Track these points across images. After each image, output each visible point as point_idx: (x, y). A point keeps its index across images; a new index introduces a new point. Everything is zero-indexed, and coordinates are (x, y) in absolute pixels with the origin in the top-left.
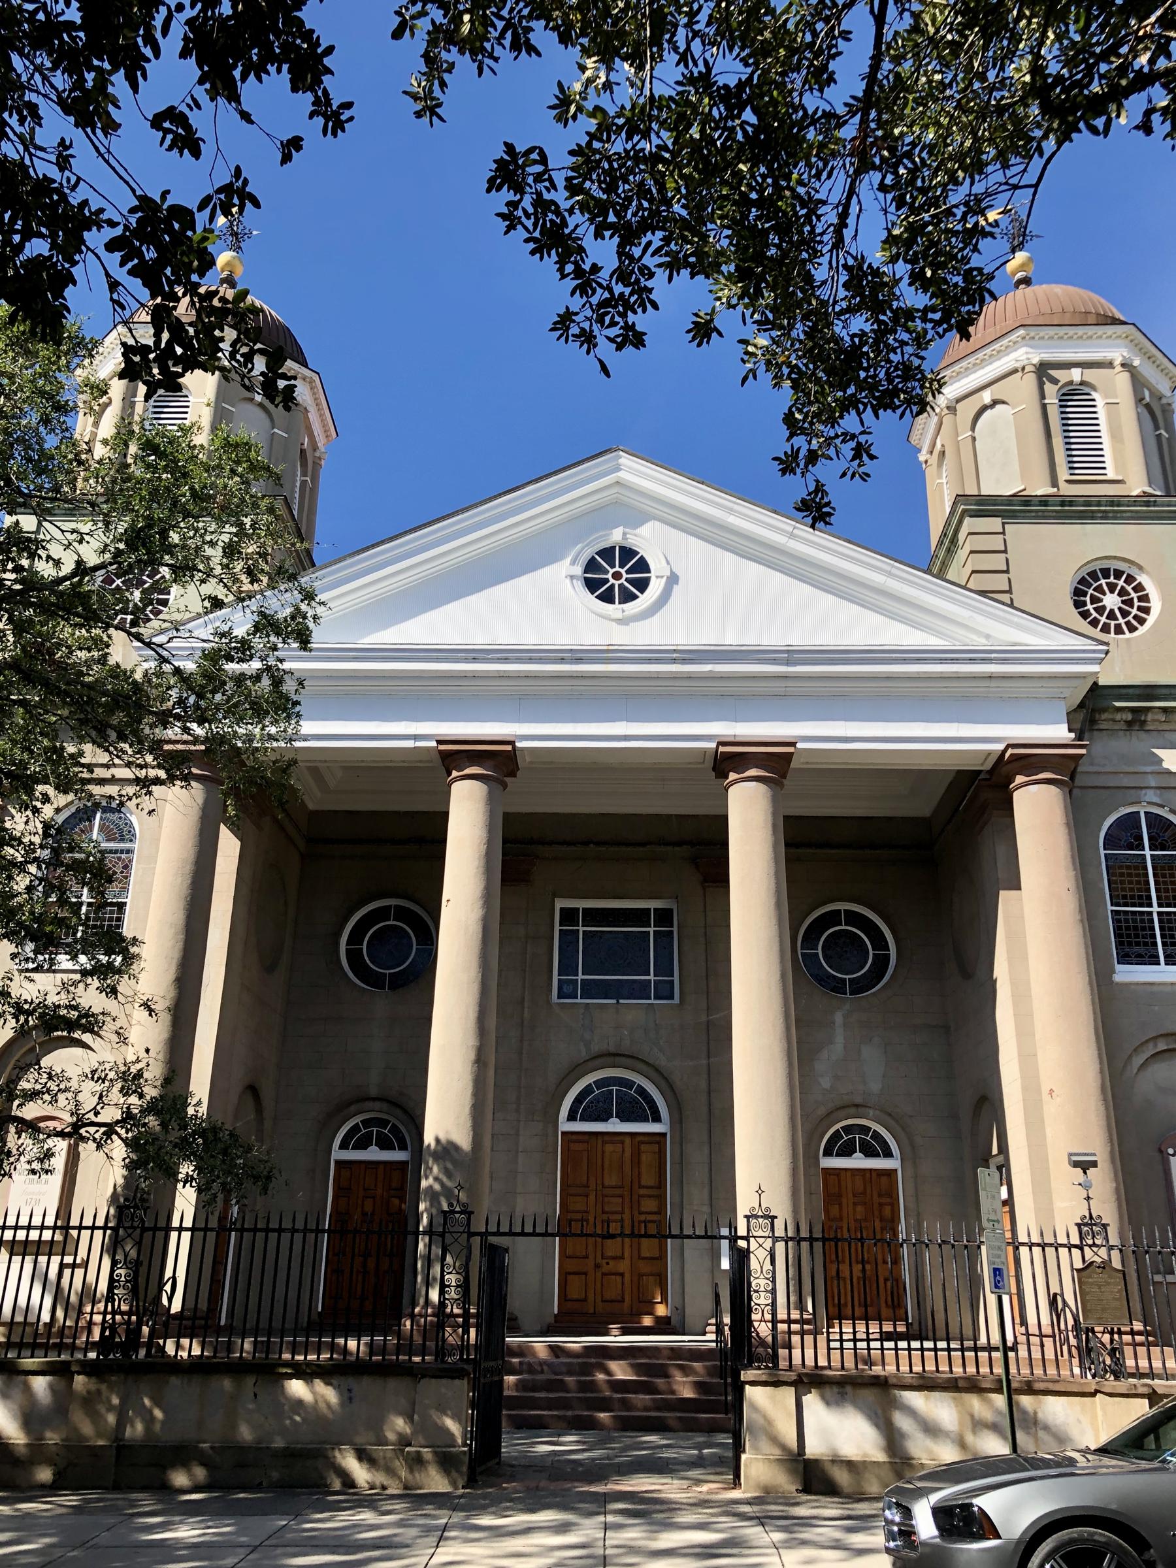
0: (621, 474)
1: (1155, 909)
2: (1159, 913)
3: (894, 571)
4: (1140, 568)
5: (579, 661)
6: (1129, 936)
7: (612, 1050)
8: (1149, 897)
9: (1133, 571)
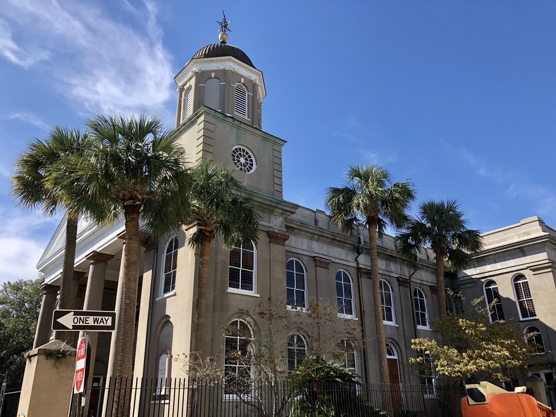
1: (241, 268)
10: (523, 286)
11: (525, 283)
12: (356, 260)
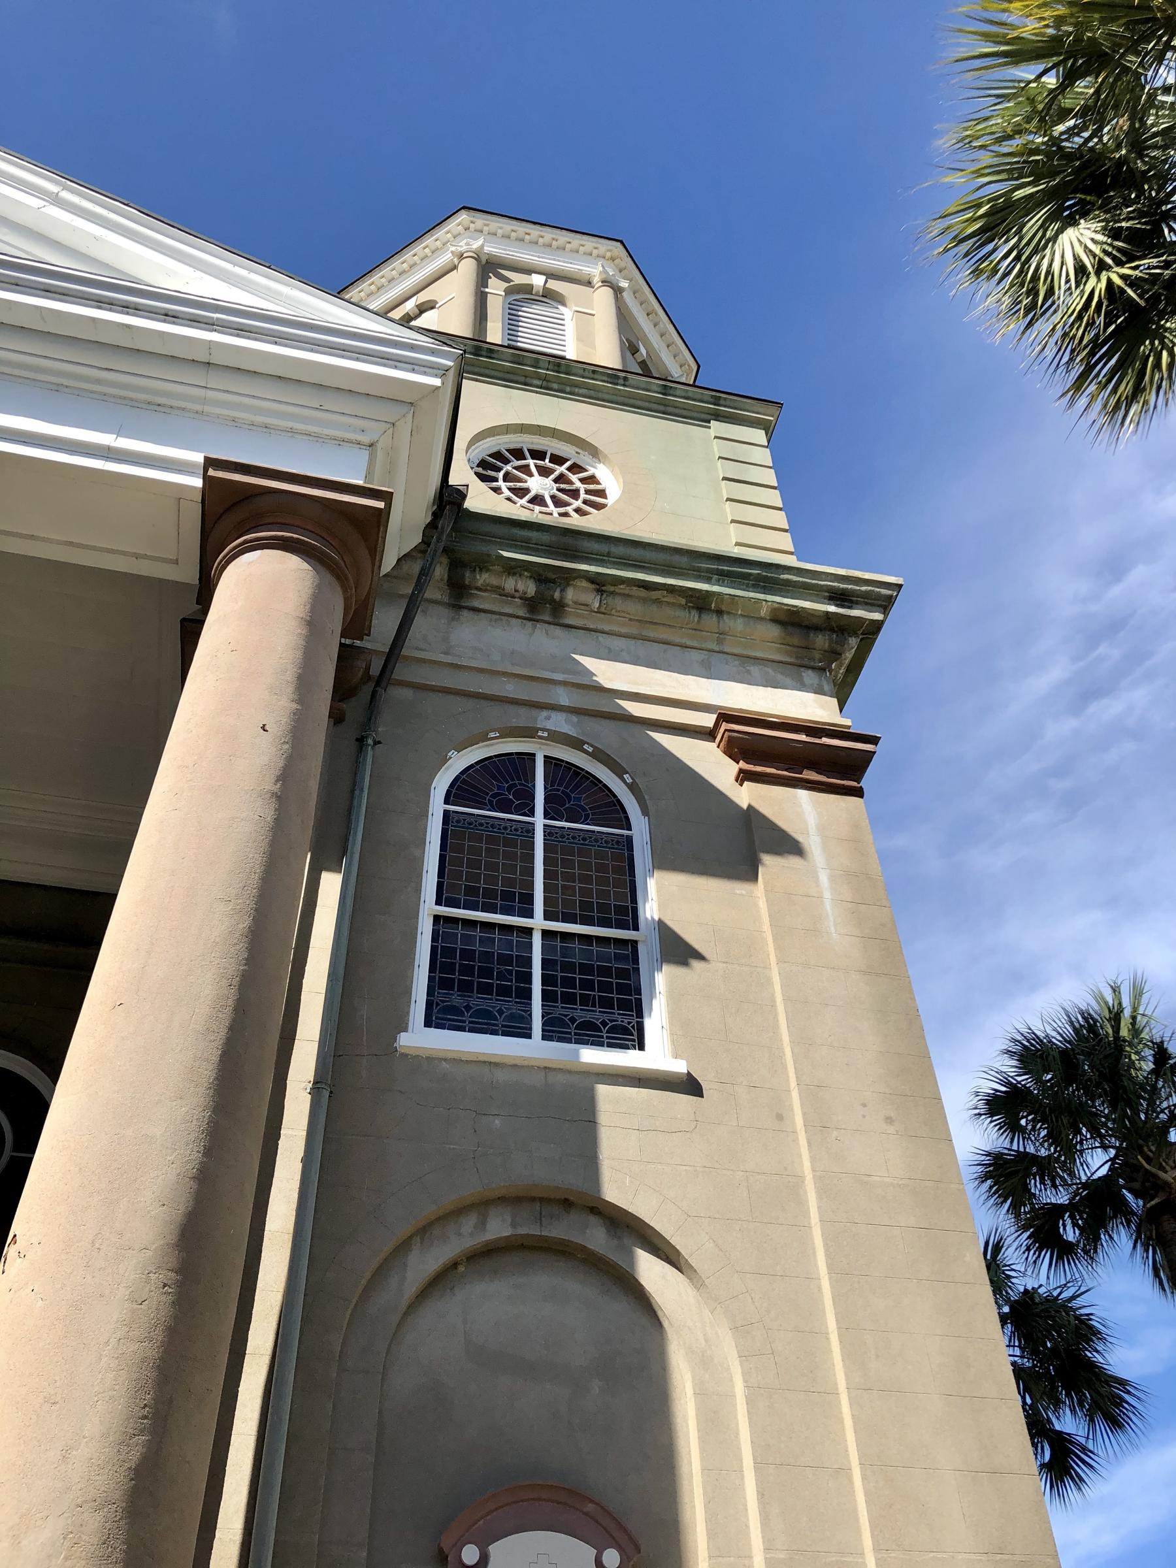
2: (546, 934)
3: (65, 195)
4: (595, 452)
6: (466, 970)
8: (529, 899)
9: (584, 459)
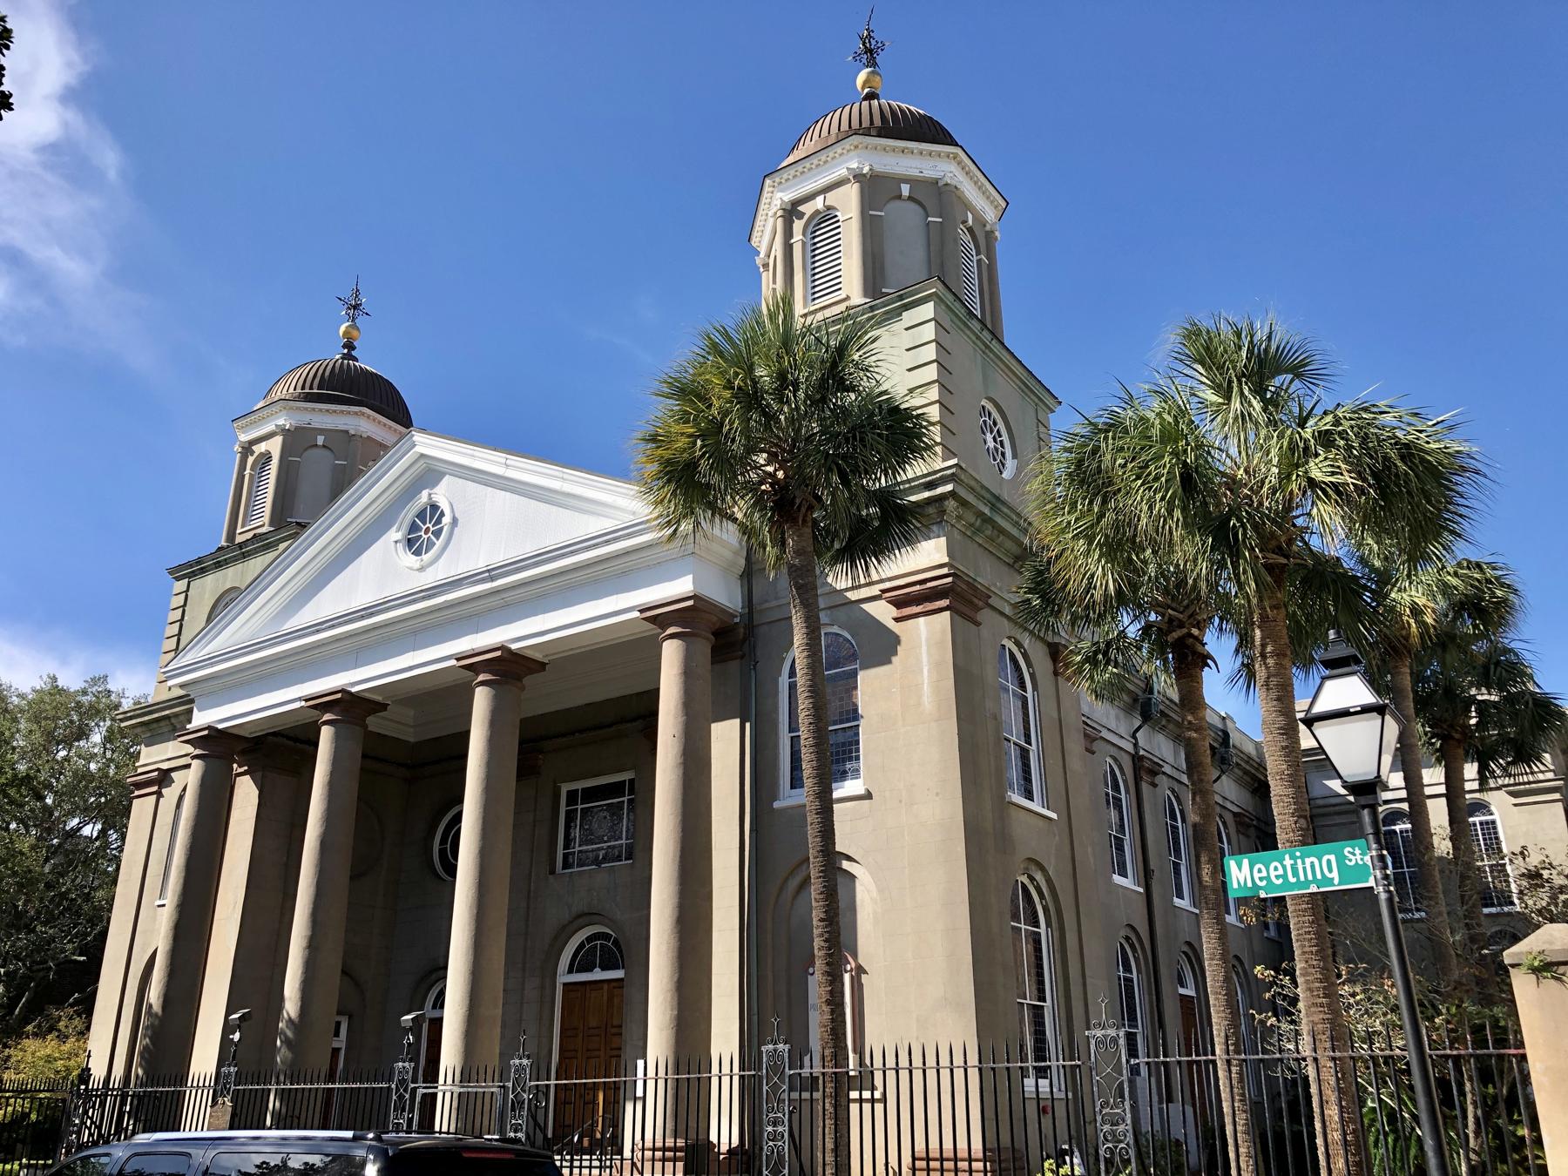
0: (419, 449)
5: (372, 615)
7: (586, 911)
10: (1482, 829)
11: (1487, 823)
12: (1134, 736)
